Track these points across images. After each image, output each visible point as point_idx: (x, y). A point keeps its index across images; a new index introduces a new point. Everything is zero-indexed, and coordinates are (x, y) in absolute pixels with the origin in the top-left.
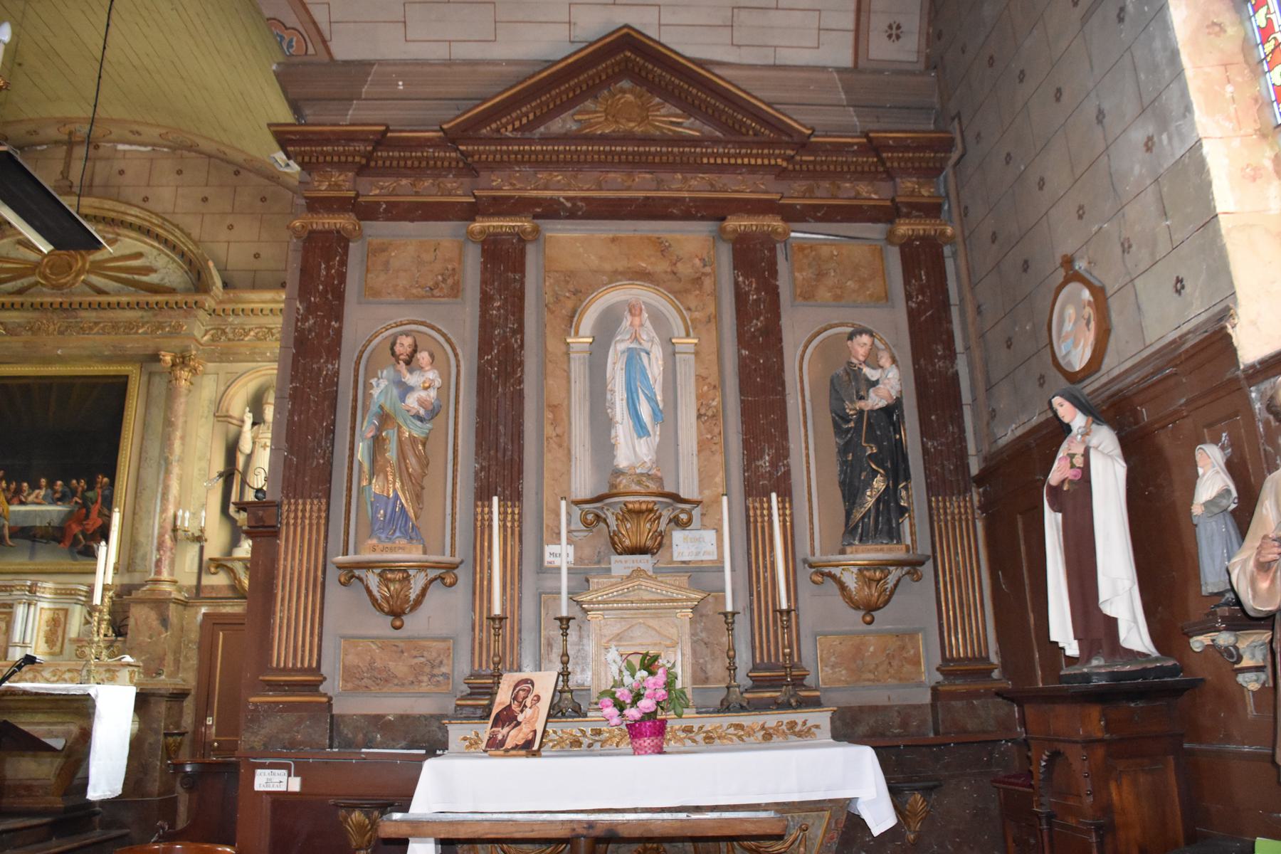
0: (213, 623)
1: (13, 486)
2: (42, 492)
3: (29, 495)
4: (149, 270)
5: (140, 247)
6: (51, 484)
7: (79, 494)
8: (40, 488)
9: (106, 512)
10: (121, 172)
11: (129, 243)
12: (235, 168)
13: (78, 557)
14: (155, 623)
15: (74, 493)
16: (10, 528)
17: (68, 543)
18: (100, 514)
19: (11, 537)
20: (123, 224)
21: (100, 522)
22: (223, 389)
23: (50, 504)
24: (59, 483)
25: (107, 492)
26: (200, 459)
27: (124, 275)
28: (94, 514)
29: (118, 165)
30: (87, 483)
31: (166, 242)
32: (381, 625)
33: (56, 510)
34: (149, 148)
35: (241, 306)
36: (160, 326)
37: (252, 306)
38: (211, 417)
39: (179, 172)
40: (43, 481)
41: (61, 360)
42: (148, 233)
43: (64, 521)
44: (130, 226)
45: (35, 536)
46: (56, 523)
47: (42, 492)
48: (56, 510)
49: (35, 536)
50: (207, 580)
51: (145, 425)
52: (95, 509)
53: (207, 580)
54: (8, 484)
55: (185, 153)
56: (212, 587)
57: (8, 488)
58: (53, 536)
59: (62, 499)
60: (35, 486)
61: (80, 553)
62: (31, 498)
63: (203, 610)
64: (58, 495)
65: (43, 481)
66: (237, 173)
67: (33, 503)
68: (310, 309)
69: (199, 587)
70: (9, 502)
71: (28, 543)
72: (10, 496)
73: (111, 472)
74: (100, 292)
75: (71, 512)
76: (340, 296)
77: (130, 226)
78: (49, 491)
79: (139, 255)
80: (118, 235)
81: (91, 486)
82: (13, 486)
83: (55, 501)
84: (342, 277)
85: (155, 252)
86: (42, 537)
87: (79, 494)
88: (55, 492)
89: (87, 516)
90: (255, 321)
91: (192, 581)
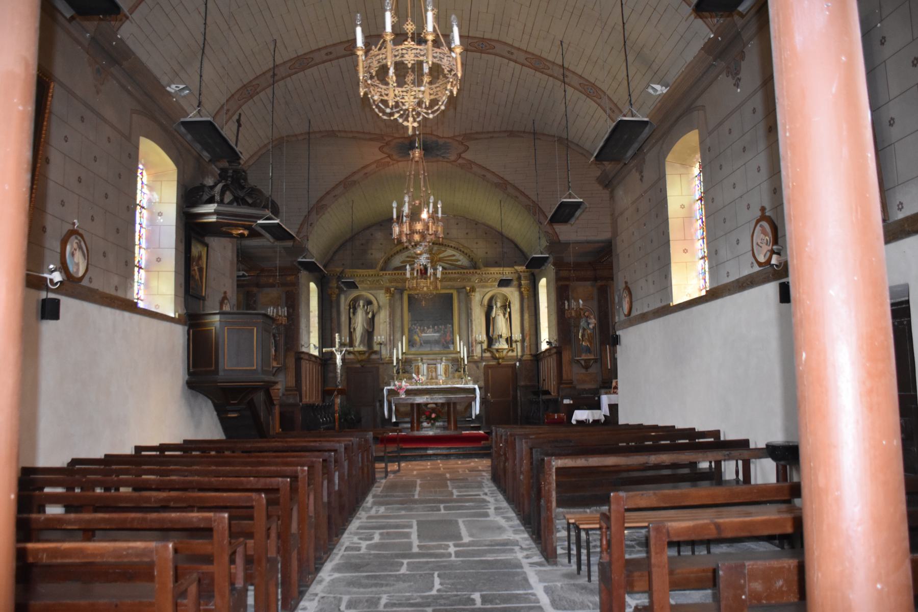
0: (487, 367)
4: (458, 260)
6: (433, 327)
11: (450, 252)
32: (583, 371)
36: (464, 279)
50: (484, 355)
53: (484, 355)
59: (438, 332)
60: (428, 328)
81: (446, 328)
90: (490, 276)
91: (480, 355)
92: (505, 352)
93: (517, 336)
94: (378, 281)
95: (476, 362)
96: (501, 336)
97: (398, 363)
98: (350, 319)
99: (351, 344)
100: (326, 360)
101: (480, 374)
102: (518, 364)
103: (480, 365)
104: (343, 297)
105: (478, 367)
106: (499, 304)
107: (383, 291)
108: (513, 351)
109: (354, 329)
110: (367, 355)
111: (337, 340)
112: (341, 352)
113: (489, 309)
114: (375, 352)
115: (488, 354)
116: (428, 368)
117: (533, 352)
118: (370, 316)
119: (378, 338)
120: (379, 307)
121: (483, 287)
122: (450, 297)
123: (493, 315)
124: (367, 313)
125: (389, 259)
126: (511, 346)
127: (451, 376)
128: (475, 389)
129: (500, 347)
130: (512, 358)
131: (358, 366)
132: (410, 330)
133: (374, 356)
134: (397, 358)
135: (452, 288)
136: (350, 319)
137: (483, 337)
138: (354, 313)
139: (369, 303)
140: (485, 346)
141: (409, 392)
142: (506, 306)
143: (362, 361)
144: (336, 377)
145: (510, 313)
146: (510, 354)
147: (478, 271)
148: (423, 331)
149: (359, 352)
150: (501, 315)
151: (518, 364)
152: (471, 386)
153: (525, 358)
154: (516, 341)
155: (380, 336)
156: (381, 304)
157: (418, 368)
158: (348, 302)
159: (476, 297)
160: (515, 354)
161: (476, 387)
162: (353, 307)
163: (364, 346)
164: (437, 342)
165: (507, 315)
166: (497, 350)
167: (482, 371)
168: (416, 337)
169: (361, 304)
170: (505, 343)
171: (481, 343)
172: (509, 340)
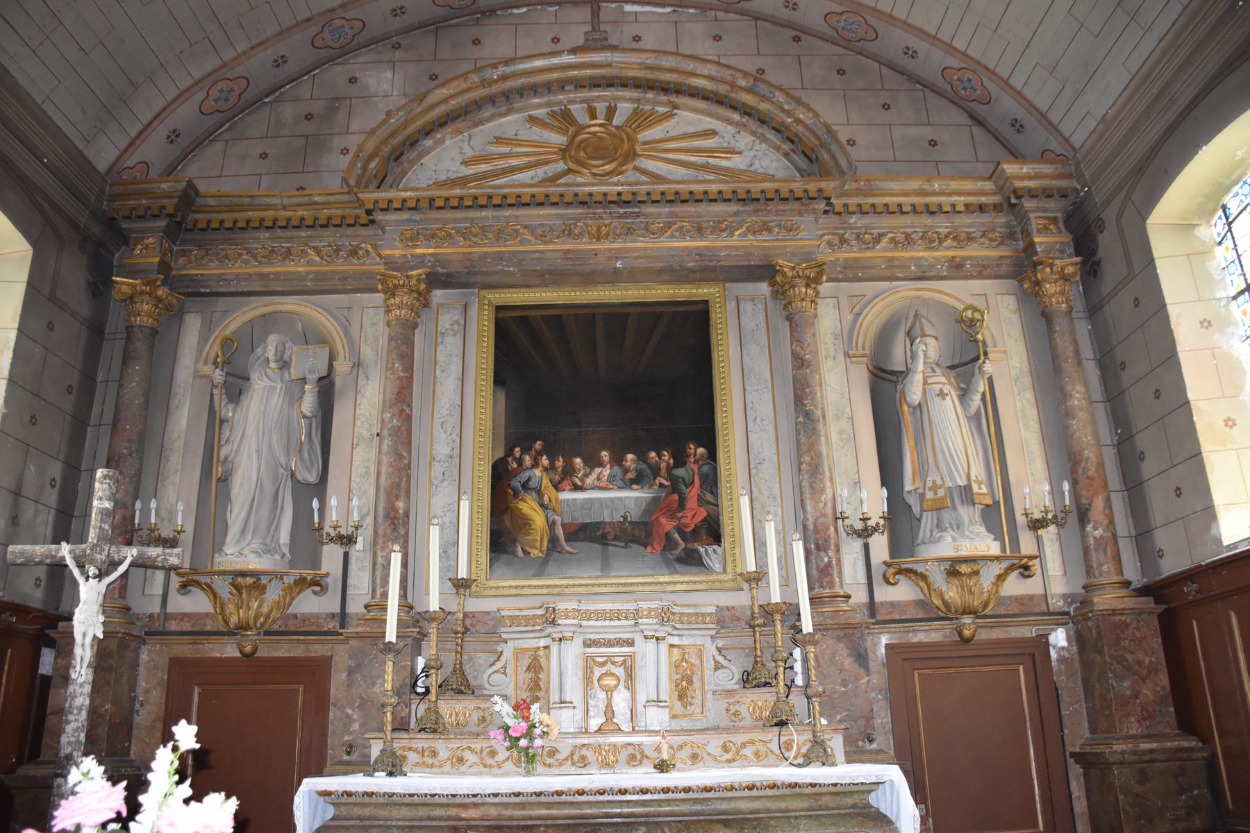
1: (560, 463)
2: (607, 472)
3: (586, 475)
5: (708, 123)
6: (617, 460)
7: (663, 473)
8: (601, 464)
9: (709, 497)
12: (794, 33)
13: (678, 567)
14: (848, 663)
15: (656, 471)
16: (564, 526)
17: (659, 548)
18: (701, 500)
19: (567, 540)
20: (679, 90)
21: (703, 514)
22: (849, 317)
23: (620, 488)
24: (630, 456)
25: (706, 469)
26: (837, 417)
27: (693, 159)
28: (692, 502)
29: (636, 29)
30: (673, 456)
31: (747, 112)
33: (633, 498)
34: (668, 10)
35: (871, 200)
37: (887, 200)
38: (841, 357)
39: (717, 38)
40: (605, 455)
41: (614, 277)
42: (720, 100)
43: (647, 512)
44: (695, 93)
45: (604, 536)
46: (634, 516)
47: (607, 472)
48: (633, 498)
49: (604, 536)
52: (692, 494)
53: (884, 594)
54: (552, 461)
55: (721, 14)
56: (892, 605)
57: (552, 467)
59: (638, 480)
60: (593, 462)
61: (680, 560)
62: (589, 481)
63: (884, 640)
64: (630, 475)
65: (605, 455)
66: (797, 39)
67: (594, 488)
69: (872, 606)
70: (557, 487)
71: (598, 547)
72: (557, 478)
73: (709, 439)
75: (655, 500)
77: (695, 93)
78: (616, 468)
79: (712, 133)
80: (675, 107)
81: (680, 461)
82: (560, 463)
83: (629, 484)
85: (732, 129)
86: (616, 538)
87: (663, 473)
88: (626, 471)
89: (682, 505)
91: (859, 596)
92: (989, 573)
96: (967, 494)
101: (873, 685)
102: (1059, 638)
104: (193, 326)
105: (861, 658)
108: (1025, 571)
111: (101, 502)
113: (885, 384)
115: (902, 592)
116: (589, 664)
118: (309, 403)
121: (852, 273)
124: (294, 390)
125: (413, 142)
127: (715, 711)
130: (1027, 608)
131: (230, 650)
132: (501, 477)
137: (872, 501)
139: (312, 337)
140: (880, 546)
142: (965, 362)
143: (243, 627)
146: (1014, 586)
147: (829, 185)
148: (565, 478)
151: (1059, 638)
153: (1106, 600)
154: (1036, 525)
155: (351, 500)
157: (536, 667)
159: (828, 317)
160: (1032, 587)
166: (954, 568)
167: (877, 677)
168: (528, 507)
170: (982, 530)
172: (997, 516)
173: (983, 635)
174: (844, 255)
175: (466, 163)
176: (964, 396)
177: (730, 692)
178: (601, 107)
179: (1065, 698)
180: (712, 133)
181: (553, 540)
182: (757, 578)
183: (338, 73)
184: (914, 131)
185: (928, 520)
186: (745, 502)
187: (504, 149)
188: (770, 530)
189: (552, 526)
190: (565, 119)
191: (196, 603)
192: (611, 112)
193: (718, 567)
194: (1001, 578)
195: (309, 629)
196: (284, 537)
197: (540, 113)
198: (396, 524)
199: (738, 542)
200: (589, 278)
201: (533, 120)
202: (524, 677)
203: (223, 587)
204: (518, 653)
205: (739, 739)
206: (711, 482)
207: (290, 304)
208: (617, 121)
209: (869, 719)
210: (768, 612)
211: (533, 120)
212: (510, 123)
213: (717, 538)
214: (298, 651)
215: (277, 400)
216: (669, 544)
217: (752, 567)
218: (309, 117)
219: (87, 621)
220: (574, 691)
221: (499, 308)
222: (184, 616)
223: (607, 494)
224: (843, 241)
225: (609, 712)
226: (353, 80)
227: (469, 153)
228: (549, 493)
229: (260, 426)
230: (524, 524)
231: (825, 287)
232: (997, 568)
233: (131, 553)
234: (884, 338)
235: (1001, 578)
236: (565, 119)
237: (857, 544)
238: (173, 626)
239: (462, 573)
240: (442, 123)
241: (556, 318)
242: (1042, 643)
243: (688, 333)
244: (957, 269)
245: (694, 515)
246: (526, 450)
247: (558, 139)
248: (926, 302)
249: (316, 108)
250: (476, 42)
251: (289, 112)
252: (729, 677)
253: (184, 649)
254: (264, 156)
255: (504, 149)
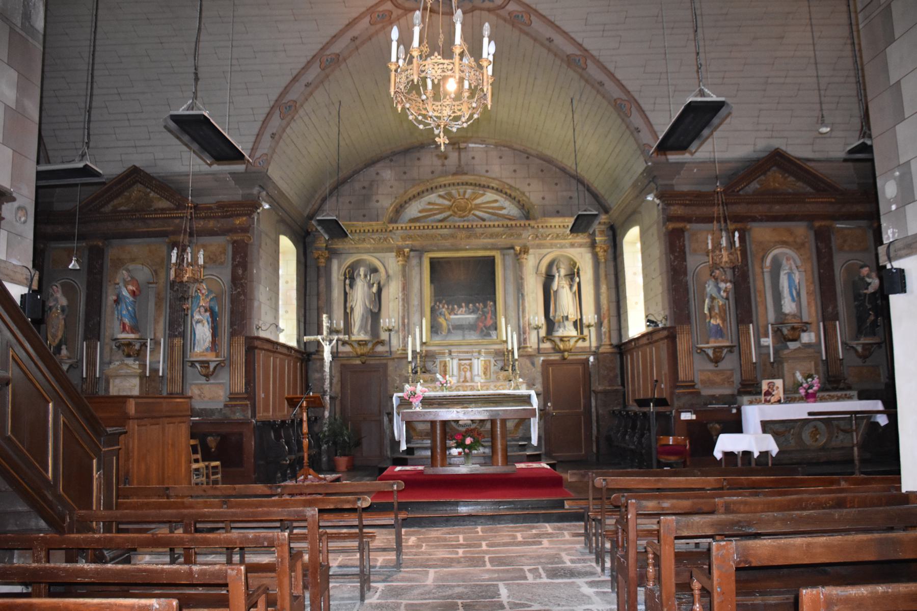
0: (546, 364)
4: (503, 208)
5: (496, 197)
6: (467, 306)
10: (473, 158)
11: (490, 196)
21: (491, 322)
28: (489, 318)
29: (471, 154)
32: (711, 366)
33: (472, 317)
36: (512, 235)
38: (535, 275)
39: (501, 158)
46: (472, 322)
50: (543, 346)
51: (505, 278)
52: (489, 316)
53: (543, 346)
58: (472, 327)
59: (473, 312)
60: (460, 306)
63: (542, 358)
68: (676, 258)
69: (539, 349)
74: (483, 220)
75: (478, 318)
76: (685, 253)
79: (496, 201)
81: (485, 306)
83: (470, 313)
84: (684, 245)
90: (549, 231)
91: (535, 346)
93: (590, 317)
94: (385, 239)
95: (530, 356)
96: (567, 318)
97: (414, 358)
98: (346, 294)
99: (347, 330)
100: (309, 355)
101: (537, 372)
102: (591, 359)
103: (536, 360)
104: (335, 264)
105: (533, 364)
106: (563, 272)
107: (394, 254)
108: (584, 339)
109: (352, 309)
110: (370, 346)
112: (330, 341)
113: (548, 279)
114: (382, 343)
115: (547, 345)
116: (460, 365)
117: (615, 341)
118: (375, 289)
119: (385, 322)
120: (388, 276)
121: (539, 246)
122: (491, 261)
123: (555, 286)
124: (371, 286)
125: (401, 206)
126: (582, 333)
127: (493, 377)
128: (529, 396)
129: (566, 334)
130: (583, 351)
131: (358, 362)
132: (433, 310)
133: (380, 349)
134: (414, 352)
135: (494, 248)
136: (346, 294)
137: (540, 320)
138: (351, 286)
139: (375, 270)
140: (543, 333)
141: (427, 402)
142: (573, 274)
143: (362, 355)
144: (322, 379)
145: (579, 284)
146: (581, 344)
147: (532, 223)
148: (452, 311)
149: (359, 343)
150: (567, 287)
151: (591, 359)
152: (523, 391)
153: (601, 350)
154: (589, 326)
155: (390, 318)
156: (391, 272)
157: (445, 366)
158: (342, 271)
160: (586, 344)
161: (533, 393)
162: (350, 277)
163: (366, 333)
164: (472, 327)
165: (575, 288)
166: (562, 339)
167: (539, 369)
168: (441, 320)
169: (362, 273)
170: (572, 328)
171: (537, 328)
172: (579, 324)
173: (571, 358)
174: (537, 242)
175: (420, 212)
176: (571, 287)
177: (497, 373)
178: (461, 191)
179: (592, 375)
180: (496, 201)
181: (449, 330)
182: (506, 342)
183: (372, 170)
184: (565, 194)
185: (556, 325)
186: (503, 320)
187: (431, 207)
188: (509, 329)
189: (448, 325)
190: (449, 196)
191: (347, 349)
192: (465, 193)
193: (495, 337)
194: (577, 341)
195: (381, 356)
196: (369, 328)
197: (442, 193)
198: (406, 328)
199: (501, 331)
200: (458, 250)
201: (440, 196)
202: (442, 368)
203: (356, 345)
204: (440, 362)
205: (498, 384)
206: (495, 312)
207: (365, 257)
208: (467, 196)
209: (534, 379)
210: (508, 351)
211: (440, 196)
212: (433, 197)
213: (496, 329)
214: (378, 362)
215: (366, 288)
216: (482, 331)
217: (504, 339)
218: (364, 188)
219: (327, 356)
220: (455, 372)
221: (431, 259)
222: (343, 352)
223: (463, 316)
224: (537, 236)
225: (465, 377)
226: (377, 174)
227: (420, 208)
228: (447, 316)
229: (360, 296)
230: (441, 325)
231: (531, 251)
232: (575, 339)
233: (336, 337)
234: (550, 265)
235: (577, 341)
236: (449, 194)
237: (536, 332)
238: (340, 355)
239: (424, 340)
240: (410, 199)
241: (448, 261)
242: (588, 360)
243: (488, 264)
244: (572, 245)
245: (489, 322)
246: (440, 302)
247: (447, 203)
248: (562, 256)
249: (366, 184)
250: (419, 159)
251: (357, 186)
252: (497, 368)
253: (345, 362)
254: (350, 202)
255: (431, 207)
